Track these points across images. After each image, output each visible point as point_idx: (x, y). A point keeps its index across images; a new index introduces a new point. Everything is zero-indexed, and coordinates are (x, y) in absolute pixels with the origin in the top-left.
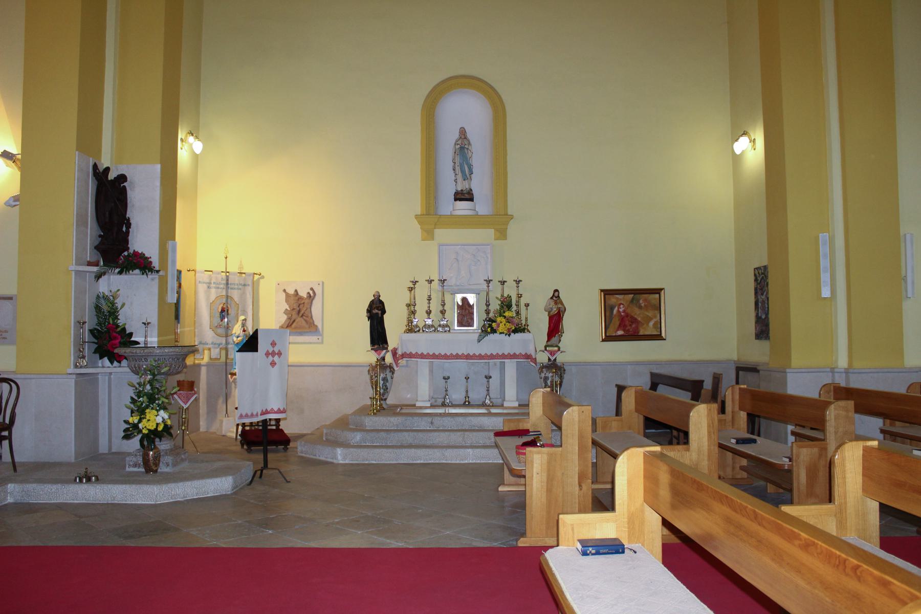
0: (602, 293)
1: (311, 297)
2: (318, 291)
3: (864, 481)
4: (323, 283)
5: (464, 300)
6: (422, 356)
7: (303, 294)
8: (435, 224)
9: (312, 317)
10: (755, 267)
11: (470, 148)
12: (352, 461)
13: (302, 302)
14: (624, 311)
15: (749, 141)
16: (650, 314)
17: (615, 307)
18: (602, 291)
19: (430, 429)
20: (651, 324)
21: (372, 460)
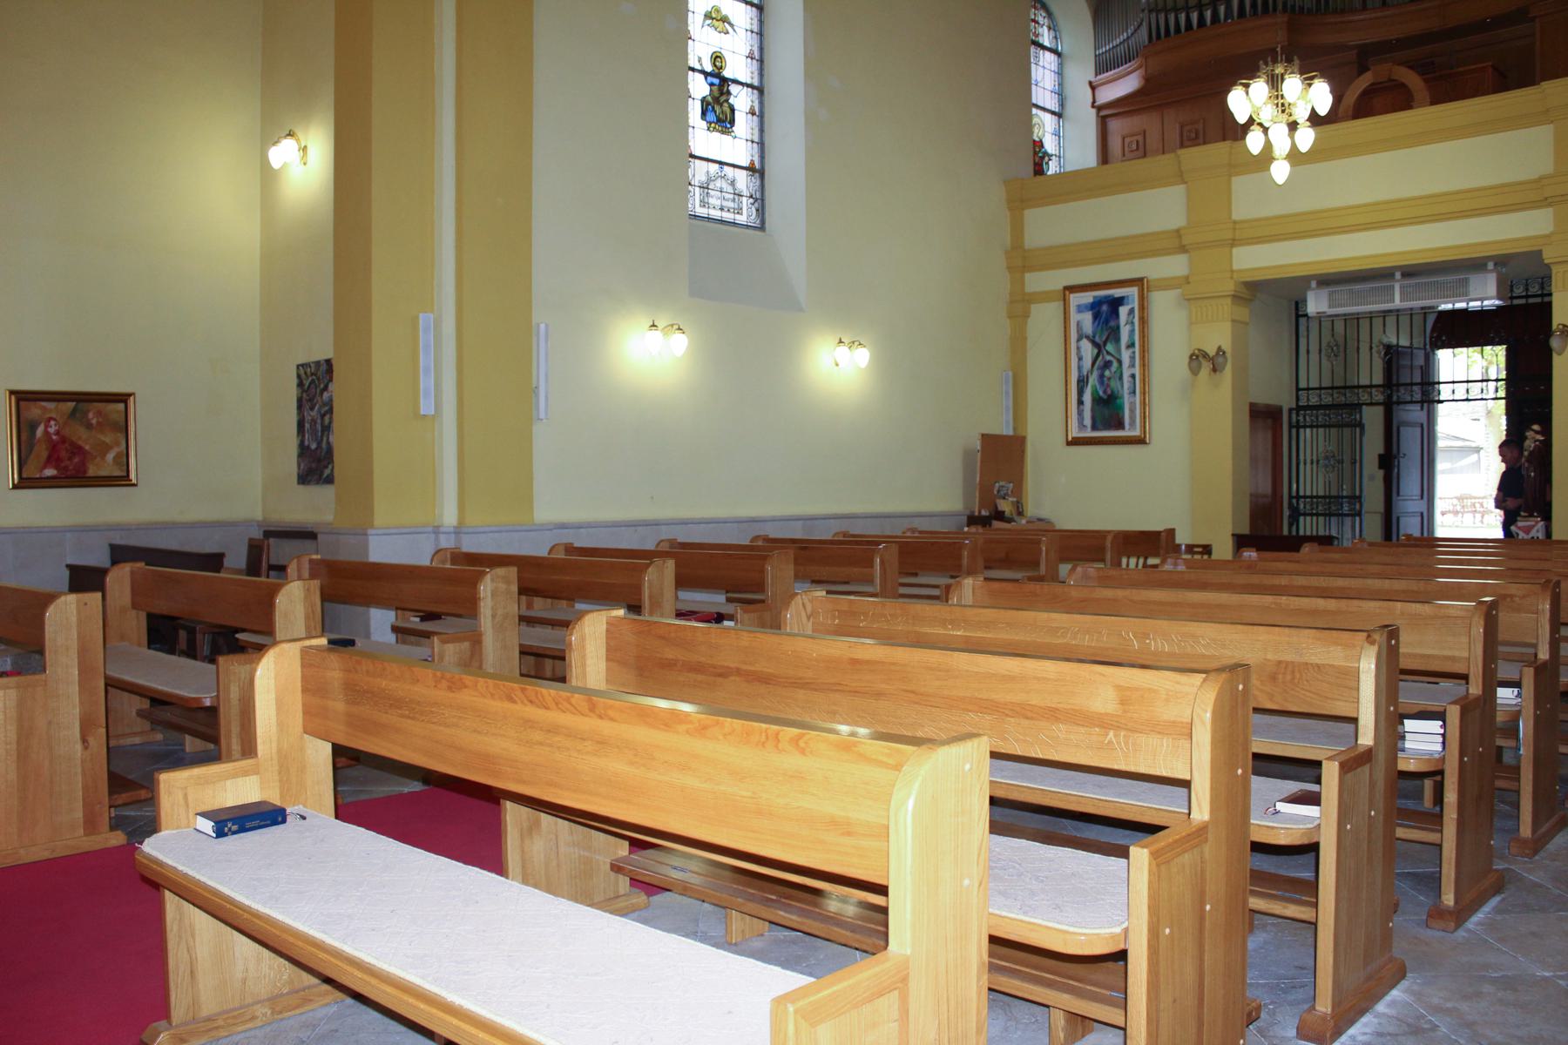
0: (13, 398)
3: (608, 669)
10: (300, 362)
14: (57, 433)
15: (297, 147)
16: (108, 439)
17: (40, 423)
18: (12, 392)
20: (110, 456)
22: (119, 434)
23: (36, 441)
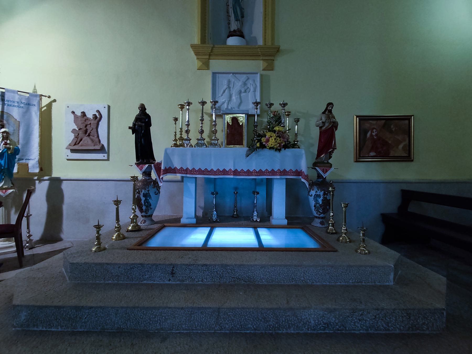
0: (358, 118)
4: (109, 107)
5: (235, 120)
6: (186, 171)
7: (90, 115)
8: (210, 55)
9: (98, 137)
13: (89, 123)
14: (376, 135)
17: (369, 131)
19: (170, 282)
20: (401, 146)
22: (406, 136)
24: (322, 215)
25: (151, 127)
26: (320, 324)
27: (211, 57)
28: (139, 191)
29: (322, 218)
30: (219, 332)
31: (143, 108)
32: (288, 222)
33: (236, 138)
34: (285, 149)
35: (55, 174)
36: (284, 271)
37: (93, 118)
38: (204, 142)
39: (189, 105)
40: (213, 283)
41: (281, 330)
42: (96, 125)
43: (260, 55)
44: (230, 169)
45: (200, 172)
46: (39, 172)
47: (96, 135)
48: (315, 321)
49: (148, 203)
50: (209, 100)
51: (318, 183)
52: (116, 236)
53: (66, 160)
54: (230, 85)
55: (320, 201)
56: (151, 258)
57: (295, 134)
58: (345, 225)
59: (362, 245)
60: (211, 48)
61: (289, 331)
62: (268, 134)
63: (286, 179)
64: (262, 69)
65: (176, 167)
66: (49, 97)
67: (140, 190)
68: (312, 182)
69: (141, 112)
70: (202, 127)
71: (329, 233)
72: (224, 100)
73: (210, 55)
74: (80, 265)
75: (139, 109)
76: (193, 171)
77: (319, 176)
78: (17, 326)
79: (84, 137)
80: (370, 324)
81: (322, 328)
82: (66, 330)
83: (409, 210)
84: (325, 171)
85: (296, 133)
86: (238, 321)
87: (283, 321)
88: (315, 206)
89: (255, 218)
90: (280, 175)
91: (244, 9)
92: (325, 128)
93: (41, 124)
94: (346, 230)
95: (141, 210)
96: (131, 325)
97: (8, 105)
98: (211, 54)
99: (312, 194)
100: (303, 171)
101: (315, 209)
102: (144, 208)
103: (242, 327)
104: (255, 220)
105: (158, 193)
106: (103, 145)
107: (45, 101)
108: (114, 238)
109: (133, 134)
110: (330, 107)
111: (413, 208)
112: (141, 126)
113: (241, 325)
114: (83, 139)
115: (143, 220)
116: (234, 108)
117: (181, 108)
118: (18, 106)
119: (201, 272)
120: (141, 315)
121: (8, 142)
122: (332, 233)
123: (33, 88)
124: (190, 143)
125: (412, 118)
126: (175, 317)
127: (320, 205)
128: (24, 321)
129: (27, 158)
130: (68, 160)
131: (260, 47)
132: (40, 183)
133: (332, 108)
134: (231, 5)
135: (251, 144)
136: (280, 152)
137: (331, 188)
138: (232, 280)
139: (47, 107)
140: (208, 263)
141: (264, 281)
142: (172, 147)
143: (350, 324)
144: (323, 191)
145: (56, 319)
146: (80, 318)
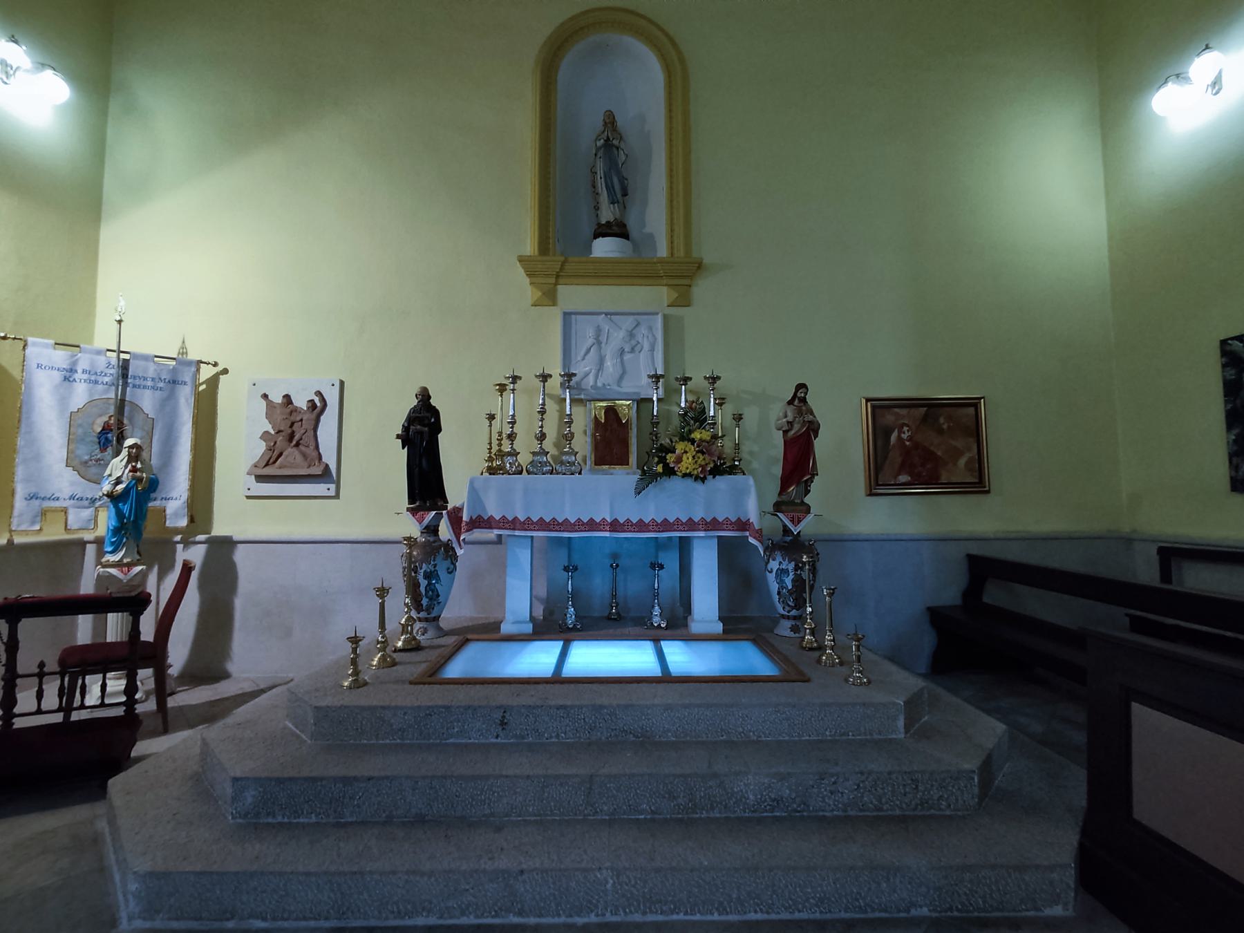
0: (869, 404)
1: (317, 408)
2: (332, 398)
4: (342, 383)
5: (611, 412)
6: (514, 524)
7: (301, 402)
8: (558, 276)
11: (622, 145)
12: (177, 919)
13: (298, 419)
14: (910, 438)
16: (959, 443)
17: (894, 431)
18: (868, 400)
19: (499, 740)
20: (962, 462)
21: (251, 916)
23: (890, 447)
24: (794, 612)
25: (442, 433)
26: (765, 801)
27: (561, 281)
28: (416, 566)
29: (795, 618)
30: (592, 818)
31: (424, 396)
32: (723, 630)
33: (615, 450)
34: (714, 477)
35: (220, 528)
36: (707, 715)
37: (308, 408)
38: (547, 458)
39: (514, 382)
40: (577, 740)
41: (697, 813)
42: (313, 422)
43: (662, 277)
44: (604, 519)
45: (542, 525)
46: (187, 525)
47: (312, 444)
48: (756, 796)
49: (432, 592)
50: (556, 371)
51: (784, 544)
52: (379, 659)
53: (245, 498)
54: (600, 338)
55: (788, 582)
56: (461, 696)
57: (734, 445)
58: (831, 631)
59: (855, 668)
60: (560, 263)
61: (712, 815)
62: (680, 447)
63: (719, 537)
64: (666, 305)
65: (491, 516)
66: (215, 365)
67: (417, 564)
68: (772, 543)
69: (420, 403)
70: (542, 427)
71: (805, 648)
72: (587, 369)
73: (558, 276)
74: (334, 709)
75: (417, 398)
76: (527, 525)
77: (786, 531)
78: (238, 815)
79: (285, 450)
80: (849, 799)
81: (768, 807)
82: (324, 821)
83: (986, 599)
84: (796, 520)
85: (737, 442)
86: (624, 799)
87: (700, 796)
88: (779, 593)
89: (656, 621)
90: (705, 530)
91: (627, 179)
92: (794, 434)
93: (196, 423)
94: (834, 640)
95: (418, 606)
96: (439, 807)
97: (134, 386)
98: (561, 274)
99: (771, 569)
100: (751, 521)
101: (779, 599)
102: (425, 602)
103: (630, 809)
104: (656, 625)
105: (452, 571)
106: (327, 465)
107: (206, 373)
108: (375, 663)
109: (403, 448)
110: (801, 393)
111: (995, 595)
112: (421, 433)
113: (629, 806)
114: (284, 453)
115: (420, 628)
116: (609, 385)
117: (499, 391)
118: (153, 388)
119: (556, 720)
120: (457, 791)
121: (139, 466)
122: (811, 649)
123: (179, 344)
124: (517, 460)
125: (980, 403)
126: (515, 793)
127: (789, 591)
128: (252, 807)
129: (164, 496)
130: (248, 497)
131: (662, 261)
132: (186, 549)
133: (806, 393)
134: (600, 173)
135: (647, 462)
136: (704, 483)
137: (805, 557)
138: (613, 734)
139: (207, 386)
140: (569, 703)
141: (670, 734)
142: (482, 474)
143: (816, 800)
144: (793, 563)
145: (308, 802)
146: (350, 798)
